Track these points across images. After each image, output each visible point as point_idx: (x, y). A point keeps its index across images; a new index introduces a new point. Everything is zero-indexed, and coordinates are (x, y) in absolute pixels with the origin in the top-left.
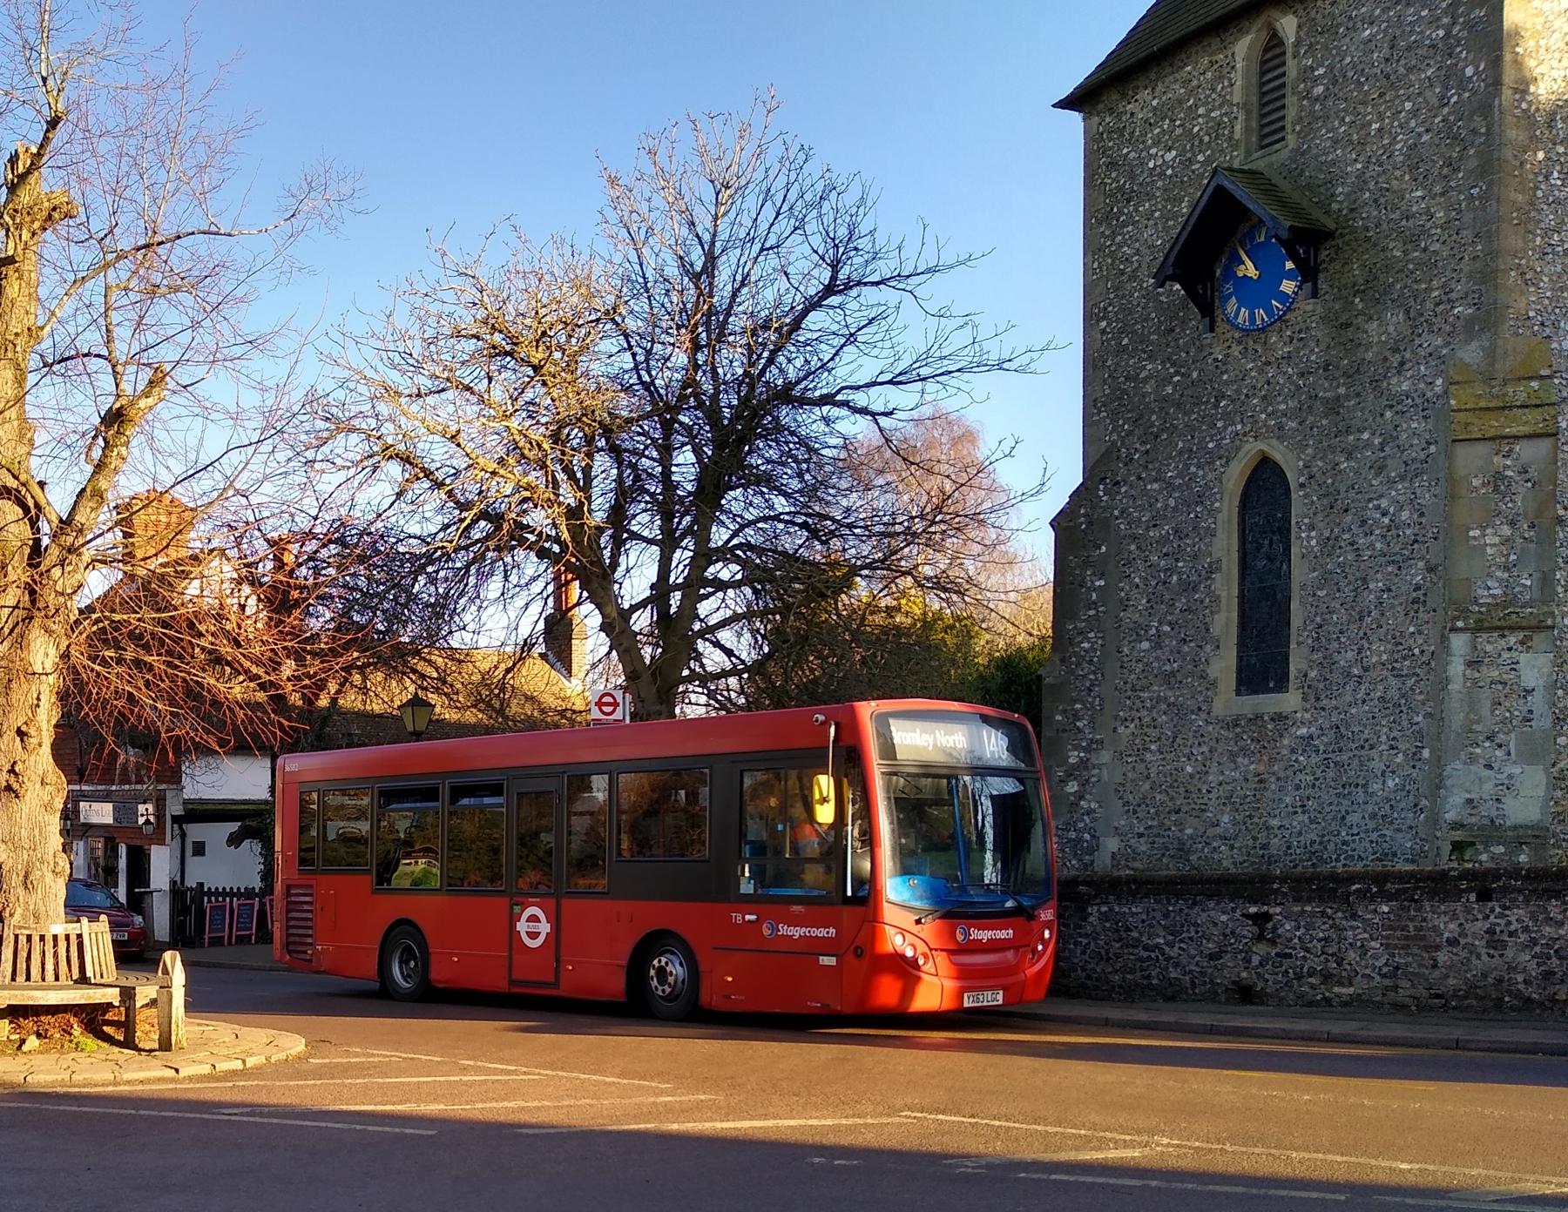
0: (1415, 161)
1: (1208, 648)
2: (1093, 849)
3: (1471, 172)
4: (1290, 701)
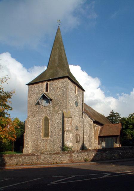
0: (60, 95)
2: (29, 151)
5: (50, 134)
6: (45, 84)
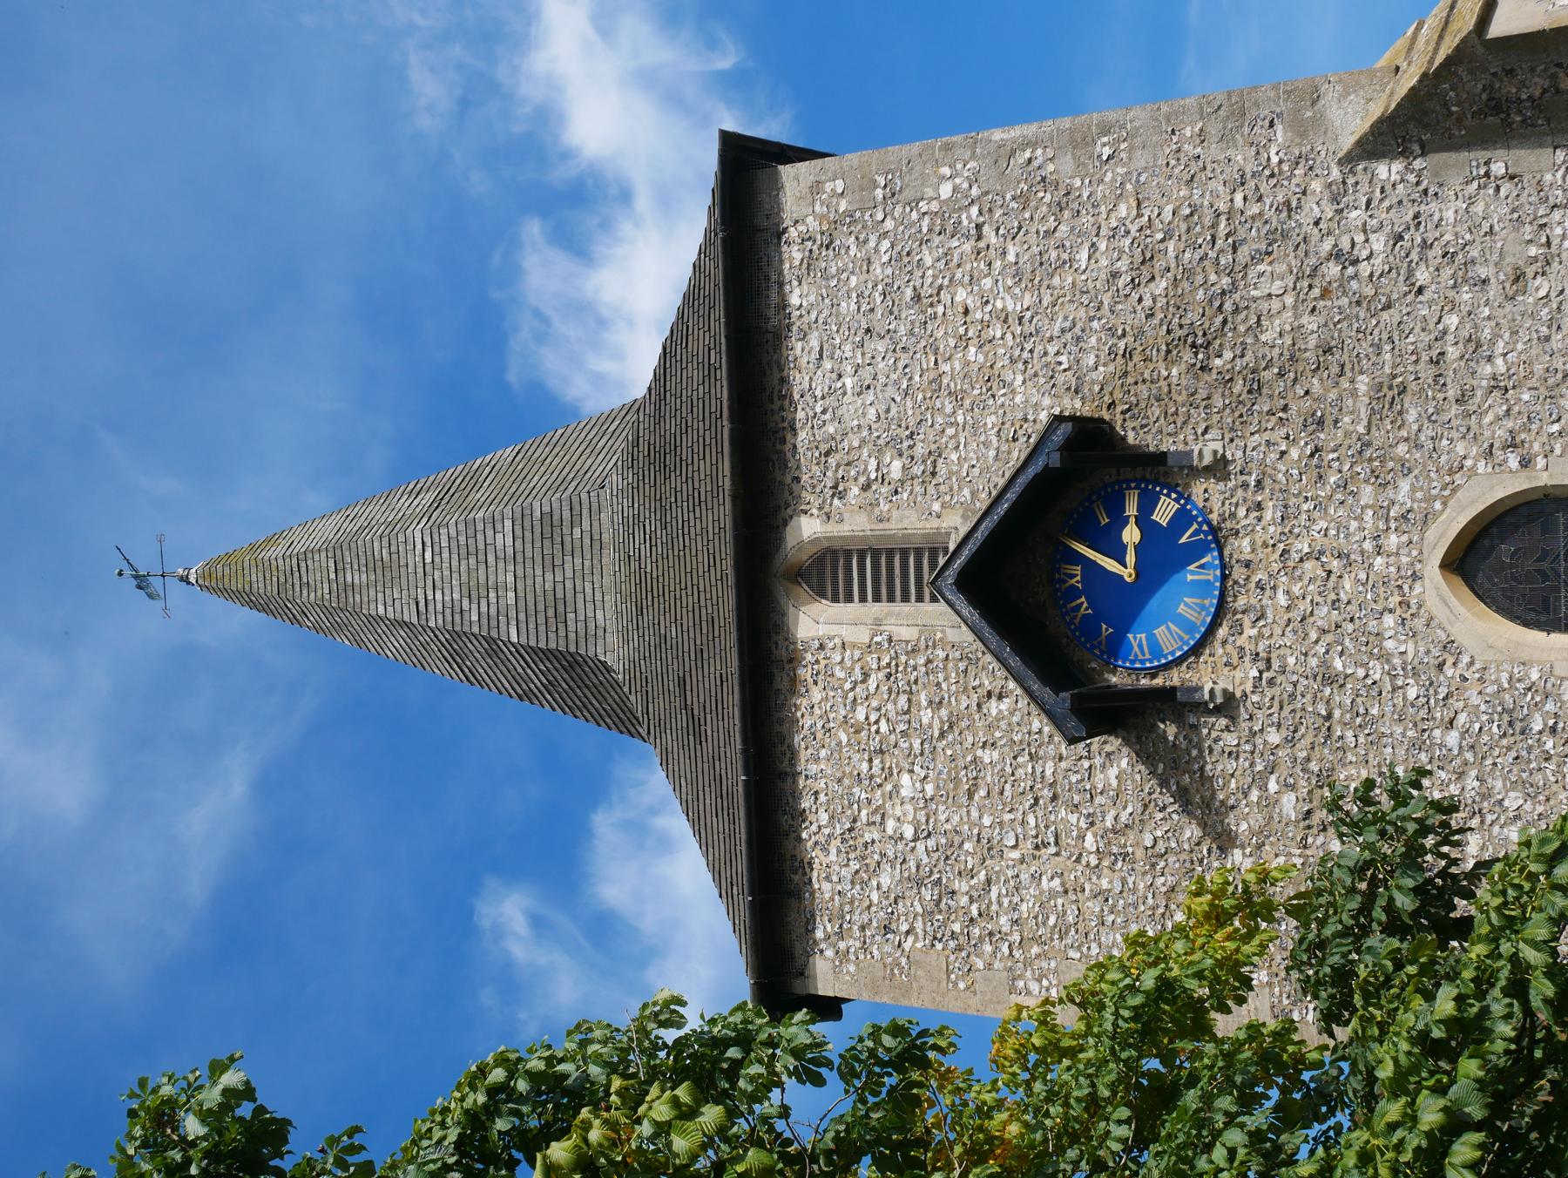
3: (1079, 165)
6: (814, 622)
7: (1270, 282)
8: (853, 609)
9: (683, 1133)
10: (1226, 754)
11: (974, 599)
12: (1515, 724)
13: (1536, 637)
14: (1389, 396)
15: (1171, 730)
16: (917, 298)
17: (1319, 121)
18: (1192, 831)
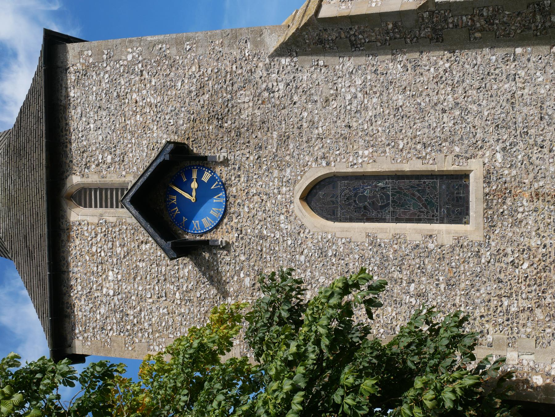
0: (162, 90)
1: (431, 246)
3: (178, 51)
4: (476, 169)
5: (448, 165)
6: (77, 215)
7: (244, 97)
8: (92, 210)
9: (5, 405)
10: (226, 264)
11: (136, 208)
12: (323, 253)
13: (330, 223)
14: (284, 139)
15: (207, 255)
16: (118, 96)
17: (262, 42)
18: (214, 291)
